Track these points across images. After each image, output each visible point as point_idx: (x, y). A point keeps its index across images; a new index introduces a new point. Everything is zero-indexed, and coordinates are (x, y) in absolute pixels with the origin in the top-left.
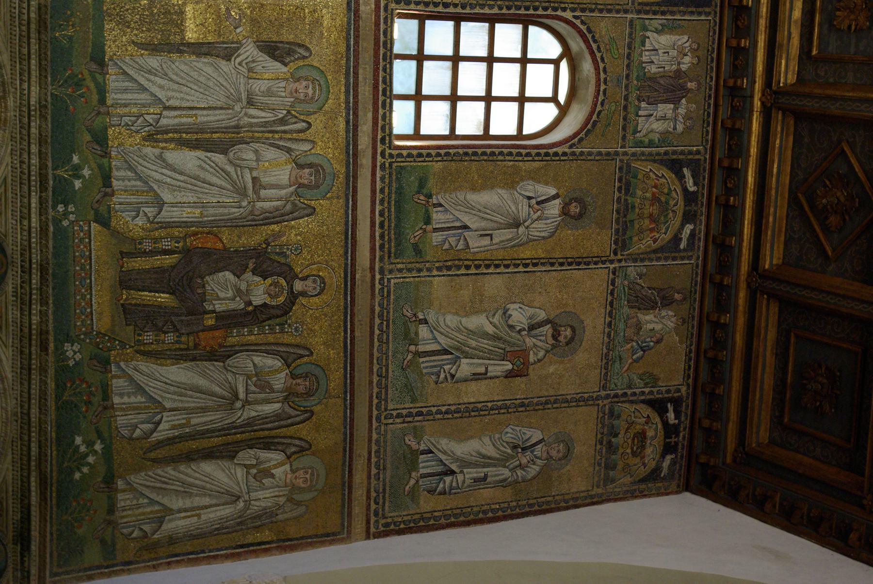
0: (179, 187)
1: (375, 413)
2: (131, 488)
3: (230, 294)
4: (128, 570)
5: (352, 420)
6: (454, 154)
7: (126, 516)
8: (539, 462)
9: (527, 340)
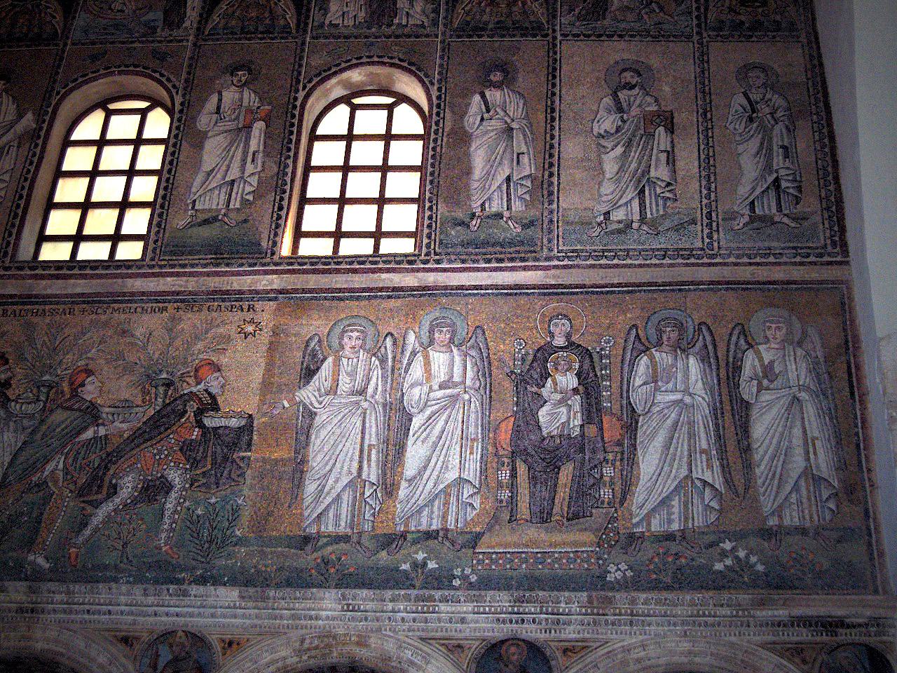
0: (443, 462)
1: (706, 260)
2: (778, 512)
3: (564, 410)
4: (874, 513)
5: (712, 283)
6: (431, 193)
7: (811, 518)
8: (768, 96)
9: (633, 113)
